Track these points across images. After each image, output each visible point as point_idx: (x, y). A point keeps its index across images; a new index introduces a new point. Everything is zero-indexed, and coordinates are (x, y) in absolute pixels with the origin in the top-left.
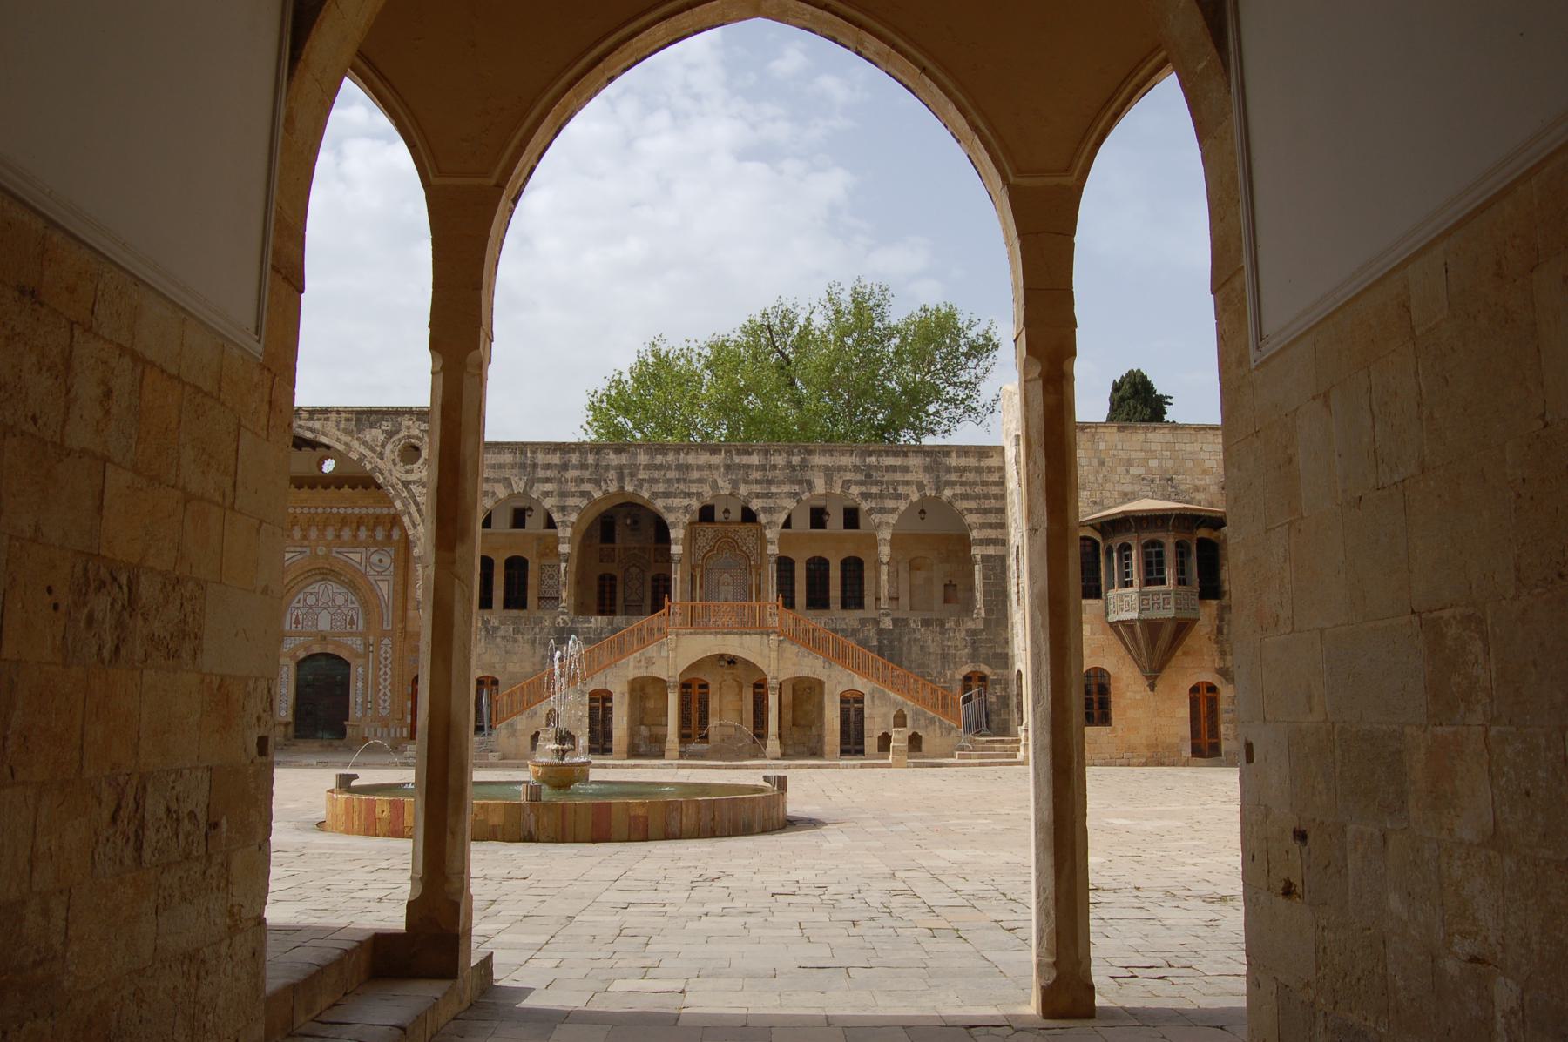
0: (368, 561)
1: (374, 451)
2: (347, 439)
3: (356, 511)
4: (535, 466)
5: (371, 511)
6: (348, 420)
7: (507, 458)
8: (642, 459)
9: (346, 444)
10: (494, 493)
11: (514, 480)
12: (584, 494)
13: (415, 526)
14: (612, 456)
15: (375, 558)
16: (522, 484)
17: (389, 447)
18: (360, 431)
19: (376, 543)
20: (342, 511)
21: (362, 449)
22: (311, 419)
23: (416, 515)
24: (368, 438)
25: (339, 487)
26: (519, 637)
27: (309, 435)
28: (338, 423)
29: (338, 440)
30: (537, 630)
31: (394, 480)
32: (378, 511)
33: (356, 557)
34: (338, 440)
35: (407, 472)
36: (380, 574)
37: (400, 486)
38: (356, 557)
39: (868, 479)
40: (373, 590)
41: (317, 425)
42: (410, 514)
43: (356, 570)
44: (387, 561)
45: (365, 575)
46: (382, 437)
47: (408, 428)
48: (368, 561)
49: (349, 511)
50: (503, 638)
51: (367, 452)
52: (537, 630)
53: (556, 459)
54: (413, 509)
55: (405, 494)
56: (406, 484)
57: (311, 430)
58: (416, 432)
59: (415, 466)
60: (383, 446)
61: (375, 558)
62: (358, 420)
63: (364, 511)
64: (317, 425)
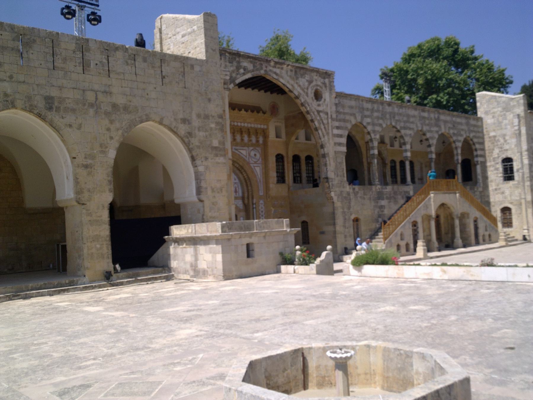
0: (249, 154)
1: (304, 92)
2: (292, 82)
3: (246, 125)
4: (363, 109)
5: (253, 126)
6: (291, 71)
7: (353, 103)
8: (396, 110)
9: (292, 86)
10: (351, 122)
11: (357, 115)
12: (380, 125)
13: (324, 136)
14: (387, 107)
15: (252, 153)
16: (360, 118)
17: (310, 90)
18: (297, 78)
19: (253, 145)
20: (239, 124)
21: (299, 89)
22: (275, 67)
23: (323, 130)
24: (301, 83)
25: (240, 110)
26: (365, 197)
27: (275, 76)
28: (287, 72)
29: (288, 82)
30: (371, 193)
31: (314, 110)
32: (256, 126)
33: (244, 152)
34: (288, 82)
35: (319, 105)
36: (255, 163)
37: (316, 113)
38: (244, 152)
39: (454, 127)
40: (253, 172)
41: (278, 71)
42: (321, 129)
43: (244, 160)
44: (258, 156)
45: (249, 163)
46: (307, 84)
47: (316, 80)
48: (249, 154)
49: (243, 124)
50: (360, 197)
51: (301, 92)
52: (371, 193)
53: (369, 106)
54: (322, 127)
55: (318, 118)
56: (319, 112)
57: (275, 73)
58: (319, 83)
59: (321, 103)
60: (307, 89)
61: (252, 153)
62: (296, 72)
63: (249, 125)
64: (278, 71)
